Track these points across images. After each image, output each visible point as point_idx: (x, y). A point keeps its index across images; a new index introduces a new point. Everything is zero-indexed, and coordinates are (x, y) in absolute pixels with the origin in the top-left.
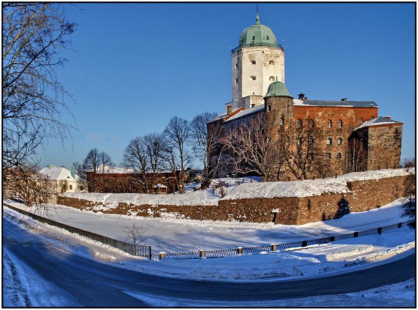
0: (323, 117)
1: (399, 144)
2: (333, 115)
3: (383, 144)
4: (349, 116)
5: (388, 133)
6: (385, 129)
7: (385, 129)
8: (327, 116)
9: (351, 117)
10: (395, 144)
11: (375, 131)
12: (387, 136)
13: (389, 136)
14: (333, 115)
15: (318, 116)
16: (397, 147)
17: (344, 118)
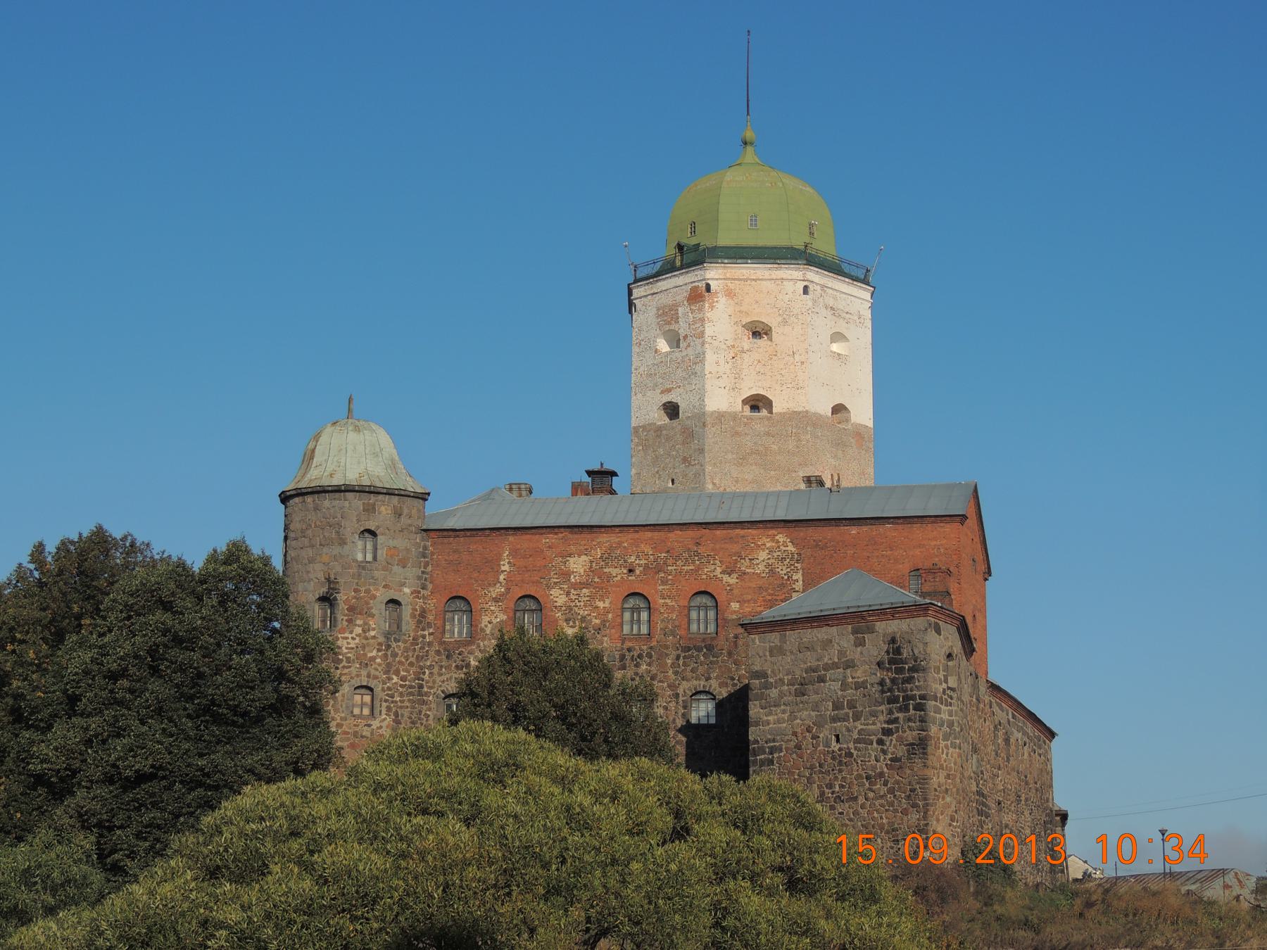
0: (596, 582)
1: (910, 736)
5: (850, 665)
6: (828, 643)
7: (828, 643)
8: (617, 572)
9: (772, 572)
10: (887, 732)
11: (777, 651)
12: (844, 686)
13: (858, 686)
15: (566, 575)
16: (901, 751)
17: (732, 580)
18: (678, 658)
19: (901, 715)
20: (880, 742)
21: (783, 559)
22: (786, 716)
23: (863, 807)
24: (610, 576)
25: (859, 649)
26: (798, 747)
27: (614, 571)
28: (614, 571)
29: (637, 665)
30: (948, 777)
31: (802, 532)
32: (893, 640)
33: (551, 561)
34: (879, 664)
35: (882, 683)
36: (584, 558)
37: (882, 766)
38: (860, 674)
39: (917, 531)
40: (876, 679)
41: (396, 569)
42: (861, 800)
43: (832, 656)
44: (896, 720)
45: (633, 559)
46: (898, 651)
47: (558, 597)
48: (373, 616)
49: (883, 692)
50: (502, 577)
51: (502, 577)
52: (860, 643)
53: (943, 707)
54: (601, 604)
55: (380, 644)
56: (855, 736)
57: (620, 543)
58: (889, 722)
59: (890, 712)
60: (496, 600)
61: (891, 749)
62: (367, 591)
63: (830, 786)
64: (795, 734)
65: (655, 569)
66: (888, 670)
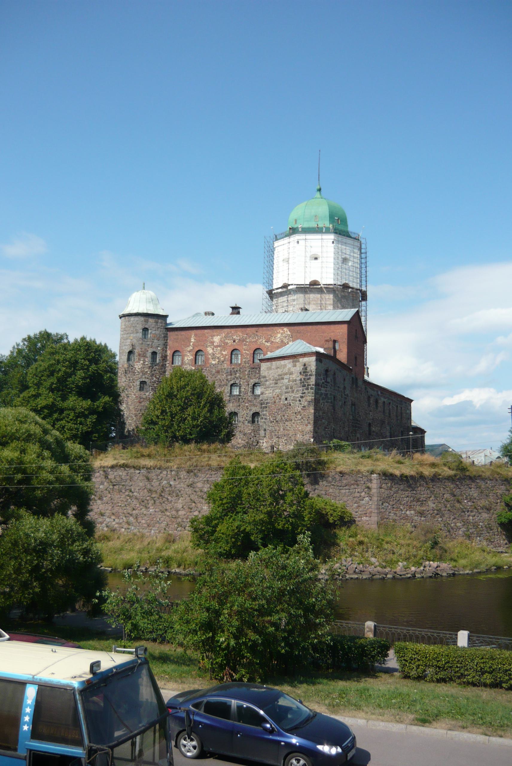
0: (223, 345)
2: (244, 341)
3: (283, 397)
4: (278, 340)
5: (291, 374)
7: (285, 366)
8: (230, 342)
10: (302, 397)
11: (269, 369)
14: (244, 341)
15: (213, 343)
16: (306, 404)
17: (268, 344)
18: (249, 371)
19: (306, 391)
20: (300, 401)
21: (286, 337)
22: (271, 391)
23: (294, 423)
24: (227, 343)
25: (294, 368)
26: (275, 402)
27: (229, 341)
28: (229, 341)
29: (236, 374)
30: (324, 413)
31: (293, 328)
32: (305, 365)
33: (208, 338)
34: (300, 373)
35: (301, 380)
36: (219, 337)
37: (299, 409)
38: (294, 377)
39: (332, 327)
40: (299, 378)
41: (155, 341)
42: (293, 421)
43: (286, 370)
44: (304, 393)
45: (235, 337)
46: (306, 369)
47: (210, 350)
48: (147, 357)
49: (301, 383)
50: (191, 344)
51: (191, 344)
52: (295, 366)
53: (323, 389)
54: (224, 353)
55: (150, 367)
56: (292, 398)
57: (231, 332)
58: (303, 393)
59: (303, 390)
60: (189, 352)
61: (303, 403)
62: (146, 349)
63: (284, 416)
64: (274, 398)
65: (242, 341)
66: (303, 375)
